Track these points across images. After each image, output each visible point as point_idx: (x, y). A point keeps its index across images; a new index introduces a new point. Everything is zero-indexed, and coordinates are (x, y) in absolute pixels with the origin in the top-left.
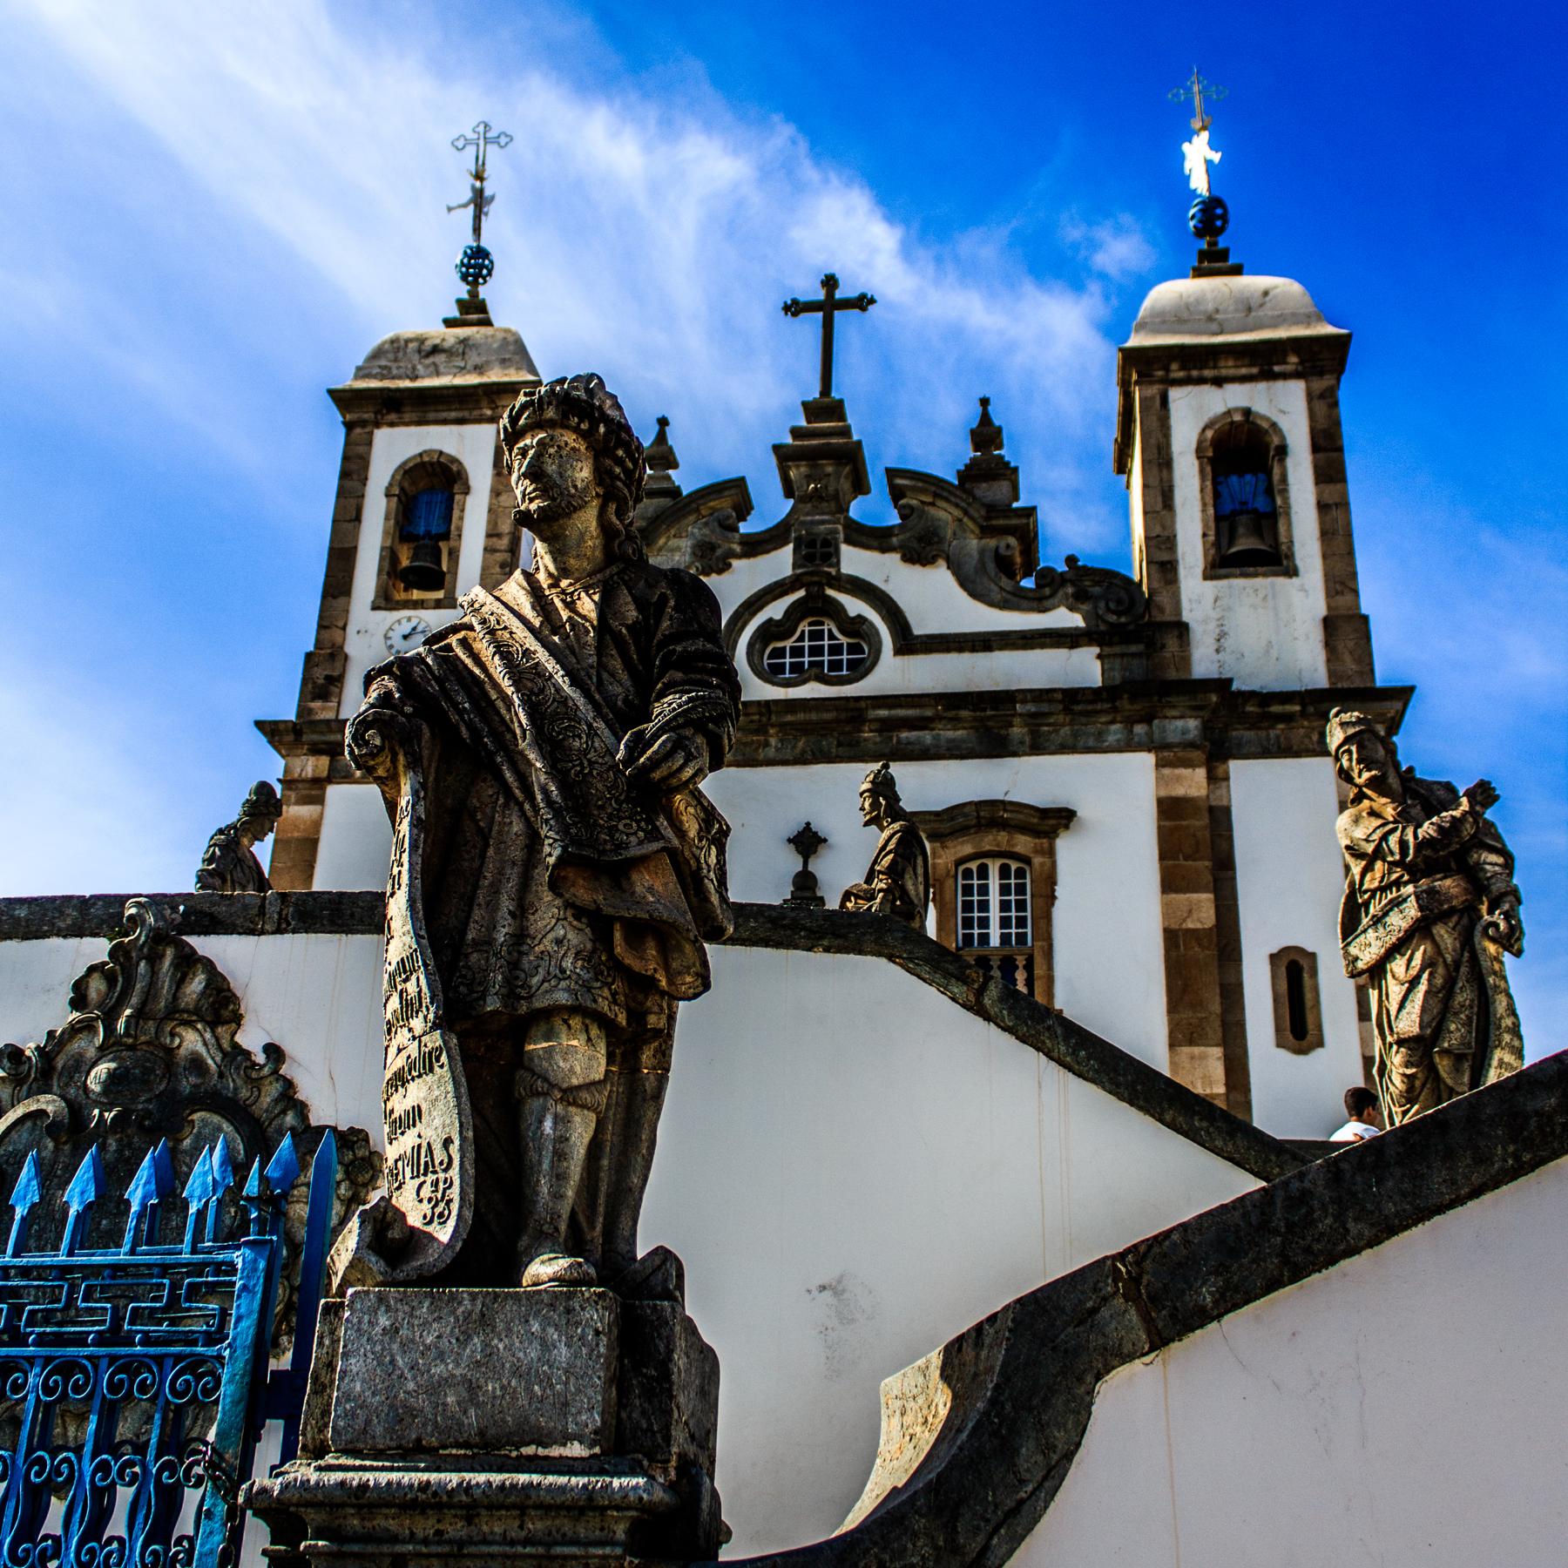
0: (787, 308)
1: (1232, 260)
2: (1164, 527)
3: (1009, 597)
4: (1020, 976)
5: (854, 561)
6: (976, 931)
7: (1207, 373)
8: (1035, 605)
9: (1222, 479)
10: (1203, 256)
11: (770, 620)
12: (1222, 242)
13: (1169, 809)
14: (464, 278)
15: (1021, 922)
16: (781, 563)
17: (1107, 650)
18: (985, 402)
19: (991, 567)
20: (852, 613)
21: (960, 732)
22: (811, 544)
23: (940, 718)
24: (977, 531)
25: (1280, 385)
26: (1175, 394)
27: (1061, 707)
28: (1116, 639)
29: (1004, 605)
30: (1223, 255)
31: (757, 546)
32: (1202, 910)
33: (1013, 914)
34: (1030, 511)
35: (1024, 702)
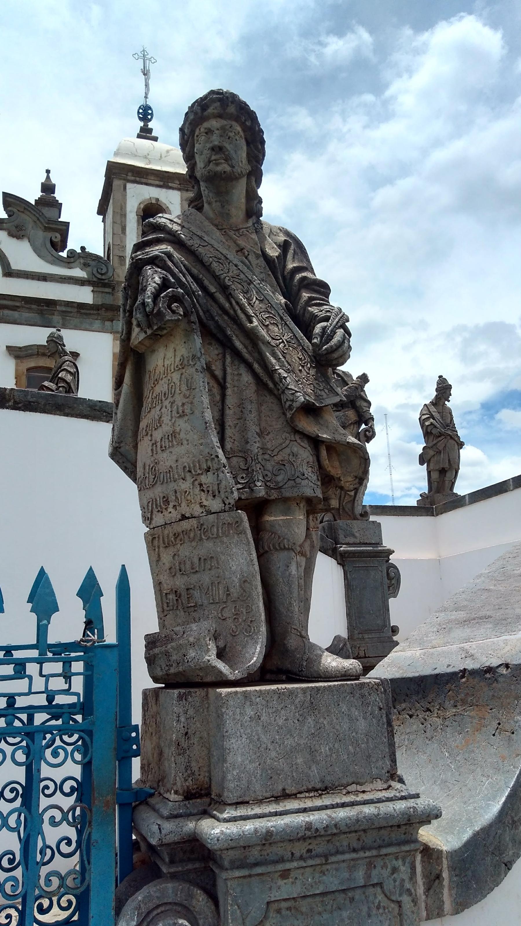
1: (154, 134)
2: (121, 242)
3: (55, 259)
7: (144, 180)
8: (66, 265)
10: (142, 129)
12: (150, 125)
17: (96, 289)
18: (48, 172)
19: (49, 245)
21: (31, 314)
23: (23, 307)
24: (43, 228)
25: (171, 191)
26: (129, 186)
27: (76, 310)
28: (100, 285)
29: (52, 263)
30: (150, 131)
34: (67, 224)
35: (61, 305)
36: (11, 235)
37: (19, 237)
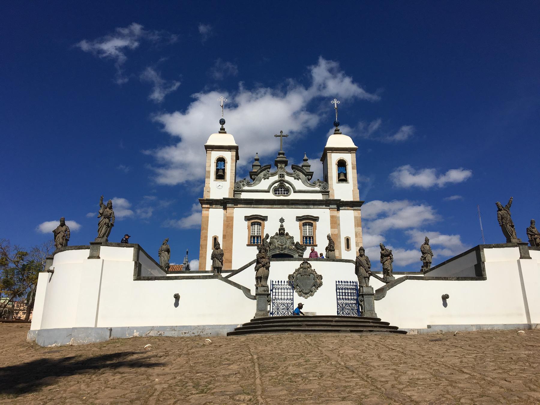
0: (275, 136)
4: (311, 239)
5: (287, 178)
6: (305, 233)
9: (339, 168)
11: (275, 187)
13: (332, 217)
14: (221, 124)
15: (311, 232)
16: (276, 178)
17: (323, 194)
20: (287, 186)
22: (281, 175)
30: (339, 130)
31: (273, 175)
32: (336, 231)
33: (310, 231)
36: (295, 179)
37: (298, 179)
